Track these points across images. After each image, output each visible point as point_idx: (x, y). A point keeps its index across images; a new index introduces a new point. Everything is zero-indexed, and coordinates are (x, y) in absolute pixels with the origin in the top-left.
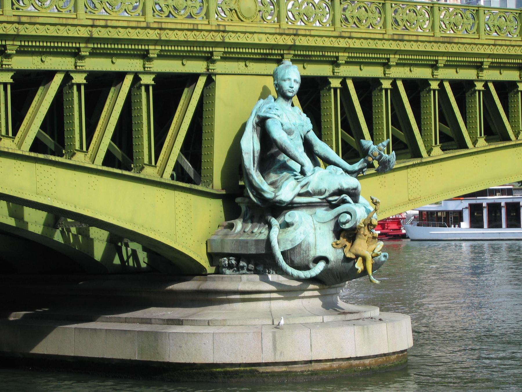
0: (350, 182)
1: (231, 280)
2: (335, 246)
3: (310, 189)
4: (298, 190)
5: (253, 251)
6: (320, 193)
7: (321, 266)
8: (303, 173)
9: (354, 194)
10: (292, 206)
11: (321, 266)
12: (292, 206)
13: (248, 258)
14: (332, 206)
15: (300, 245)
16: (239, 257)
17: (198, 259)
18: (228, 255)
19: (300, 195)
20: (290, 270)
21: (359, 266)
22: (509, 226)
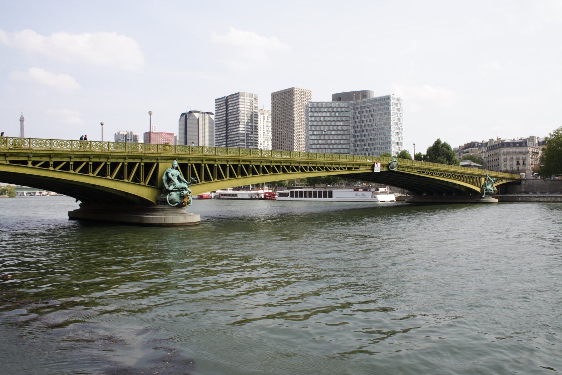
0: (186, 186)
1: (159, 206)
2: (180, 200)
3: (176, 187)
4: (174, 187)
5: (163, 200)
6: (178, 188)
7: (177, 204)
8: (175, 184)
9: (185, 189)
10: (172, 191)
11: (177, 204)
12: (172, 191)
13: (163, 201)
14: (179, 191)
15: (172, 199)
16: (161, 201)
17: (153, 202)
18: (159, 201)
19: (174, 189)
20: (170, 204)
21: (184, 204)
22: (319, 197)
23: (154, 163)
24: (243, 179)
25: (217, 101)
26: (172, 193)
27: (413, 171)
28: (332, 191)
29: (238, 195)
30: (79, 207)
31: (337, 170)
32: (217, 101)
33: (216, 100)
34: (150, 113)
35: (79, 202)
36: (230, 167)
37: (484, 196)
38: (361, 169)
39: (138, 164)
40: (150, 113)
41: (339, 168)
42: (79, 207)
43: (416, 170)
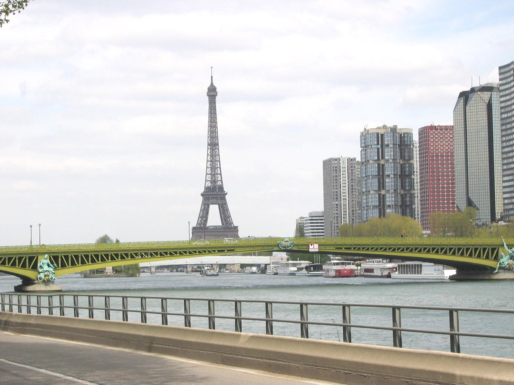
10: (41, 272)
12: (41, 272)
23: (35, 257)
24: (103, 264)
25: (502, 71)
26: (41, 273)
27: (326, 248)
28: (421, 265)
29: (375, 271)
30: (21, 283)
31: (175, 255)
32: (502, 71)
33: (500, 68)
34: (40, 225)
35: (22, 280)
36: (92, 256)
37: (496, 271)
38: (236, 250)
39: (24, 258)
40: (40, 225)
41: (197, 251)
42: (21, 283)
43: (333, 247)
